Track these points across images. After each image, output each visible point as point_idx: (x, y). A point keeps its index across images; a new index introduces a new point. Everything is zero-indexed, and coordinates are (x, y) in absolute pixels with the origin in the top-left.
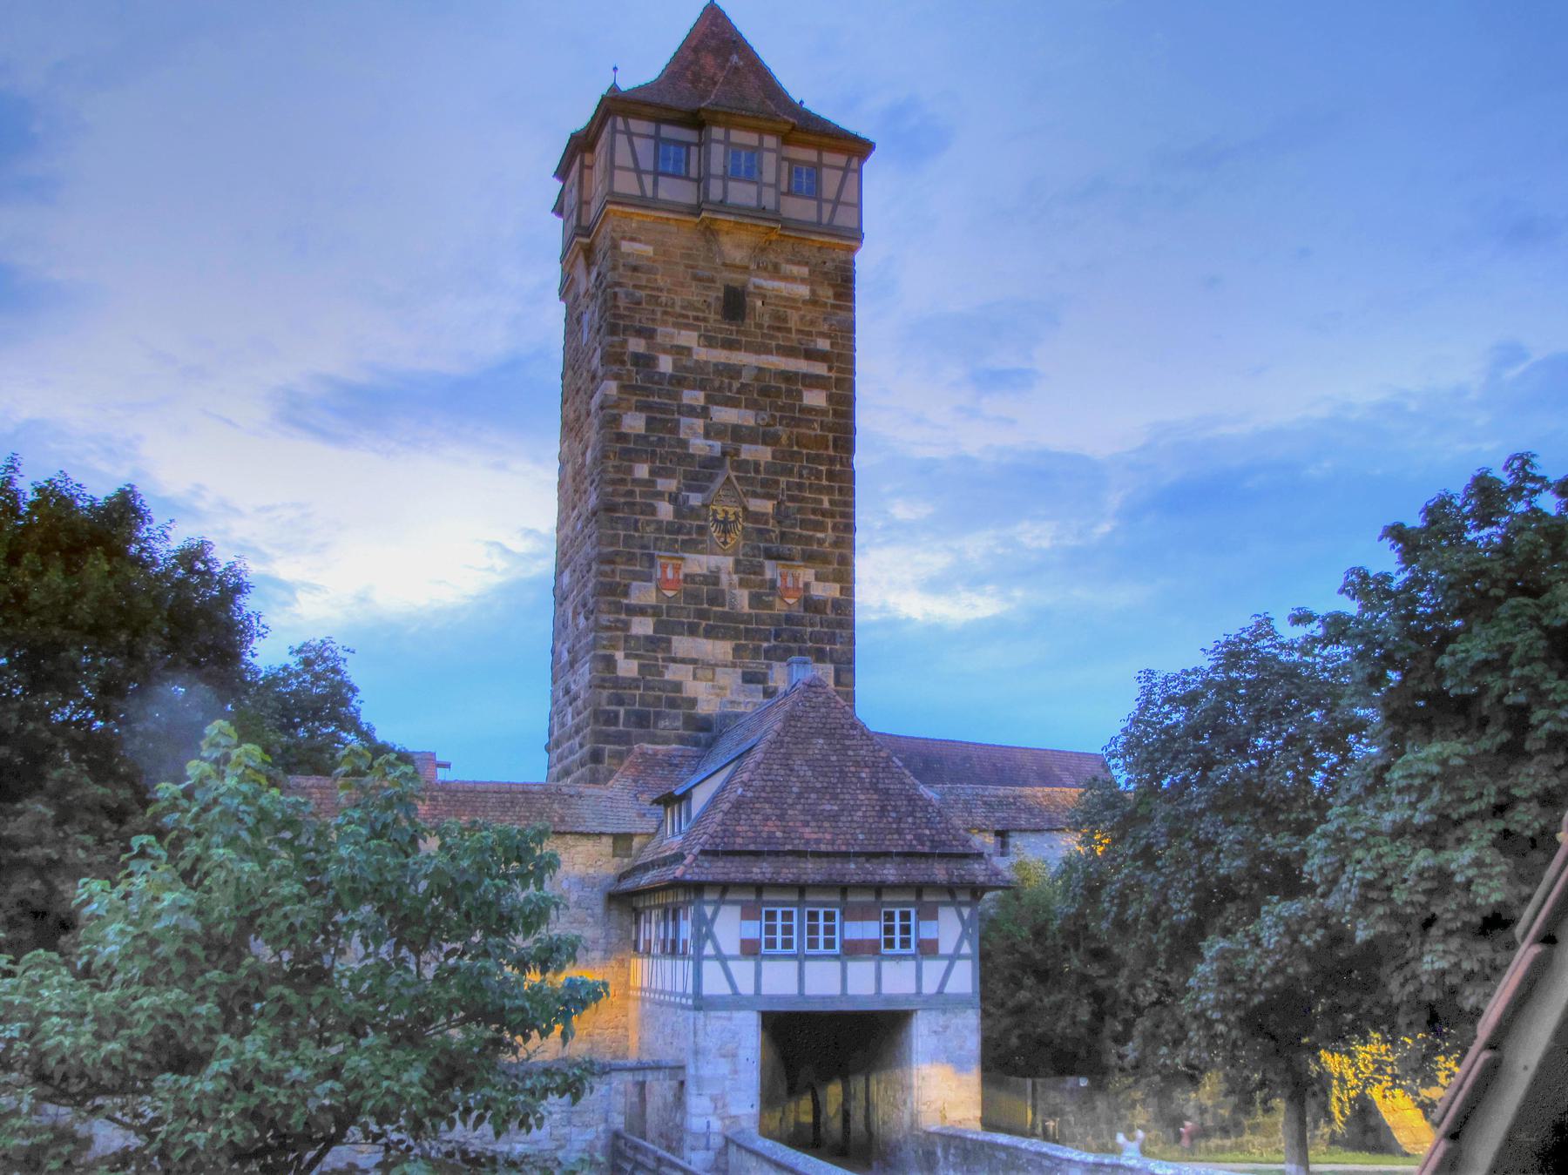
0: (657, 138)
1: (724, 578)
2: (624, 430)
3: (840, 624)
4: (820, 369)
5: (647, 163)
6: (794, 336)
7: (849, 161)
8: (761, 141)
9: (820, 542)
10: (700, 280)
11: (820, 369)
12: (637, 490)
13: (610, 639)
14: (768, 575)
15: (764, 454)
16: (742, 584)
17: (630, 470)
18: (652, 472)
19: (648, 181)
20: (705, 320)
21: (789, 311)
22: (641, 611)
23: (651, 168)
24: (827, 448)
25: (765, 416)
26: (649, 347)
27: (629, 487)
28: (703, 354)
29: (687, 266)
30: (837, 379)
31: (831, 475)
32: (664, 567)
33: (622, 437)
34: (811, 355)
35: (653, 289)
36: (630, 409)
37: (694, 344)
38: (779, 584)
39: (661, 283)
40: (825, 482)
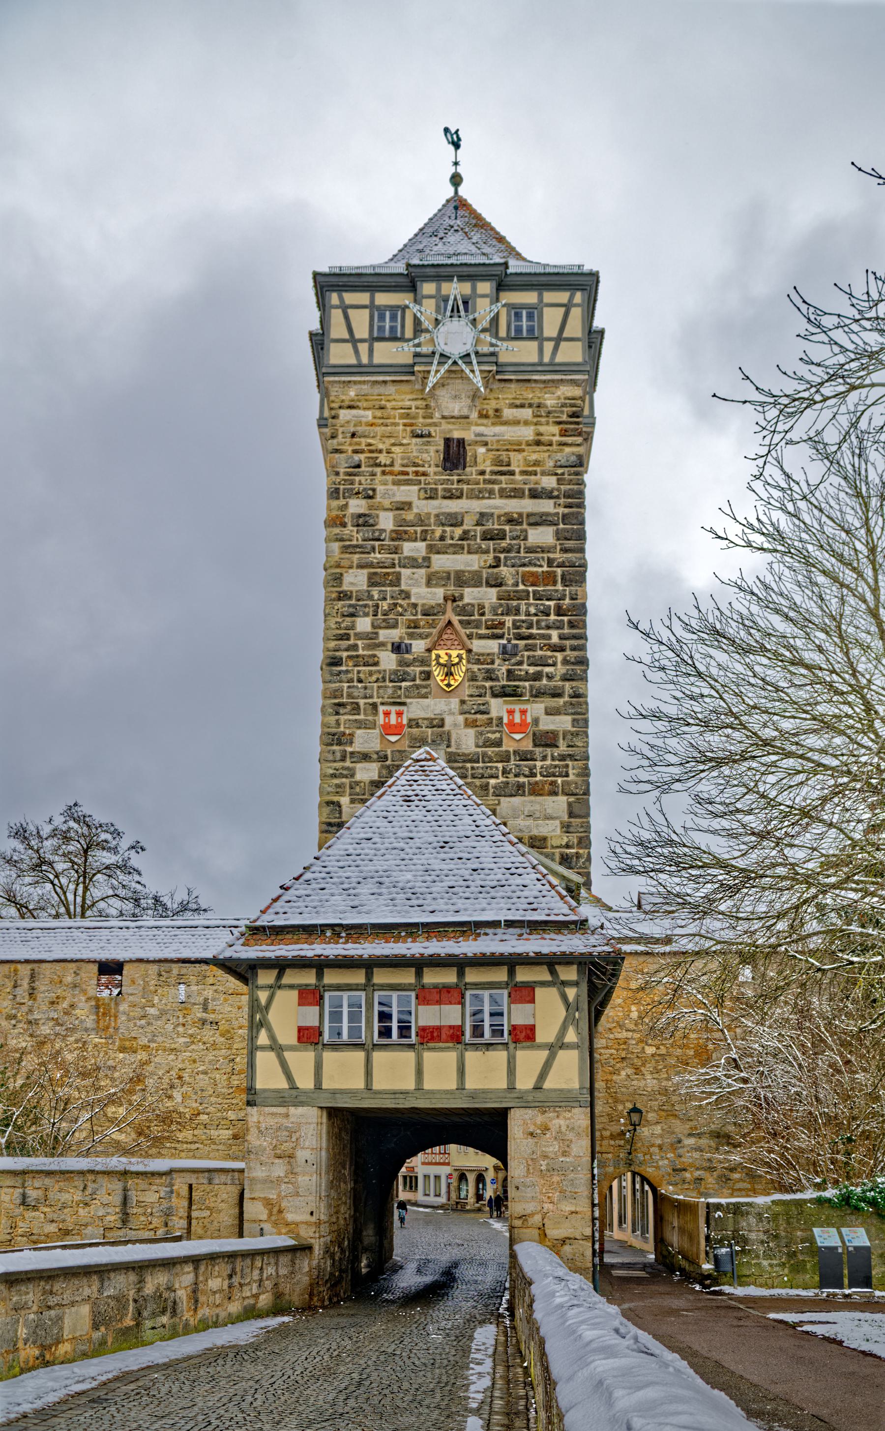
0: (371, 306)
1: (448, 721)
2: (345, 587)
3: (571, 757)
4: (546, 506)
5: (362, 332)
6: (518, 477)
7: (571, 298)
8: (474, 288)
9: (550, 677)
10: (421, 436)
11: (546, 506)
12: (359, 643)
13: (338, 786)
14: (494, 714)
15: (490, 596)
16: (468, 724)
17: (353, 627)
18: (373, 626)
19: (363, 348)
20: (424, 474)
21: (512, 454)
22: (365, 757)
23: (366, 335)
24: (555, 583)
25: (490, 558)
26: (370, 508)
27: (352, 642)
28: (422, 506)
29: (405, 425)
30: (564, 516)
31: (559, 612)
32: (387, 714)
33: (344, 596)
34: (535, 494)
35: (371, 451)
36: (351, 567)
37: (414, 499)
38: (505, 721)
39: (381, 446)
40: (553, 617)
